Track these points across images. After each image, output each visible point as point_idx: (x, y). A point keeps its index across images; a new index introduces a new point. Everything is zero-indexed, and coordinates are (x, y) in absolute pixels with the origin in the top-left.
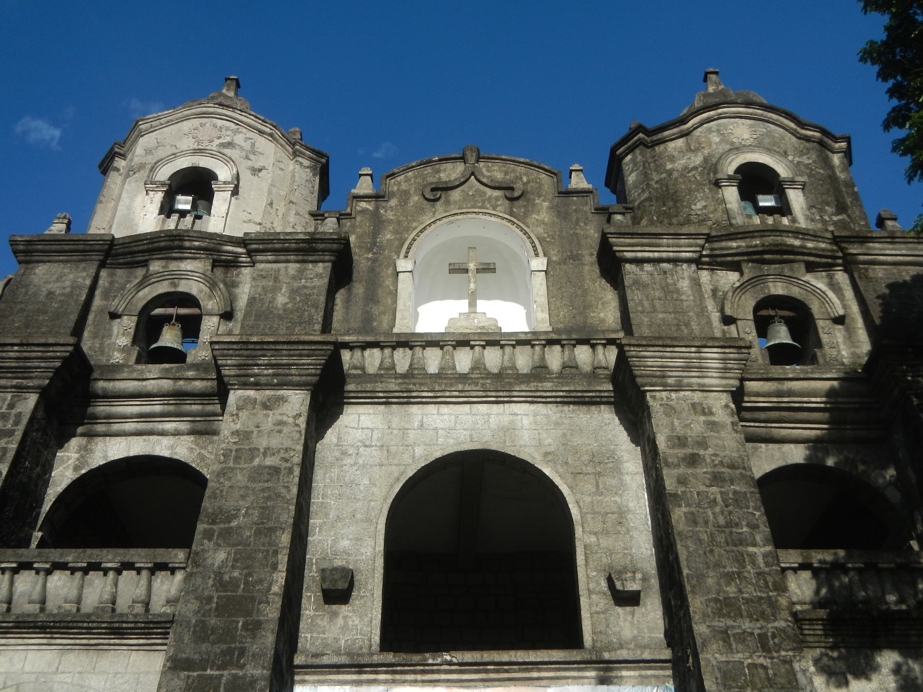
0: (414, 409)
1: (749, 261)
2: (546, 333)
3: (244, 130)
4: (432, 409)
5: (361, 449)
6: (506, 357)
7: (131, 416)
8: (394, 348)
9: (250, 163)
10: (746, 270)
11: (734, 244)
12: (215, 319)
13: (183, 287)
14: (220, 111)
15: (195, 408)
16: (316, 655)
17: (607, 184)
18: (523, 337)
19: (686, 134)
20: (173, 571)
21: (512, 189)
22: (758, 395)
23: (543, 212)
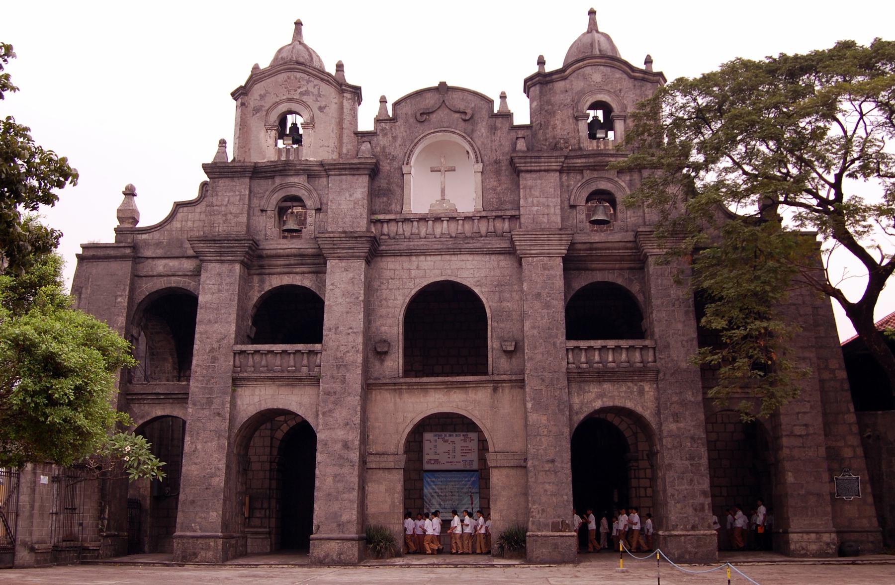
0: (414, 258)
1: (587, 170)
2: (480, 212)
3: (312, 79)
4: (422, 258)
5: (390, 281)
6: (460, 227)
7: (280, 266)
8: (403, 222)
9: (318, 104)
10: (585, 175)
11: (579, 161)
12: (313, 212)
13: (293, 192)
14: (298, 66)
15: (309, 261)
16: (376, 379)
17: (525, 92)
18: (468, 215)
19: (565, 78)
20: (317, 353)
21: (465, 113)
22: (580, 250)
23: (482, 129)
